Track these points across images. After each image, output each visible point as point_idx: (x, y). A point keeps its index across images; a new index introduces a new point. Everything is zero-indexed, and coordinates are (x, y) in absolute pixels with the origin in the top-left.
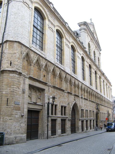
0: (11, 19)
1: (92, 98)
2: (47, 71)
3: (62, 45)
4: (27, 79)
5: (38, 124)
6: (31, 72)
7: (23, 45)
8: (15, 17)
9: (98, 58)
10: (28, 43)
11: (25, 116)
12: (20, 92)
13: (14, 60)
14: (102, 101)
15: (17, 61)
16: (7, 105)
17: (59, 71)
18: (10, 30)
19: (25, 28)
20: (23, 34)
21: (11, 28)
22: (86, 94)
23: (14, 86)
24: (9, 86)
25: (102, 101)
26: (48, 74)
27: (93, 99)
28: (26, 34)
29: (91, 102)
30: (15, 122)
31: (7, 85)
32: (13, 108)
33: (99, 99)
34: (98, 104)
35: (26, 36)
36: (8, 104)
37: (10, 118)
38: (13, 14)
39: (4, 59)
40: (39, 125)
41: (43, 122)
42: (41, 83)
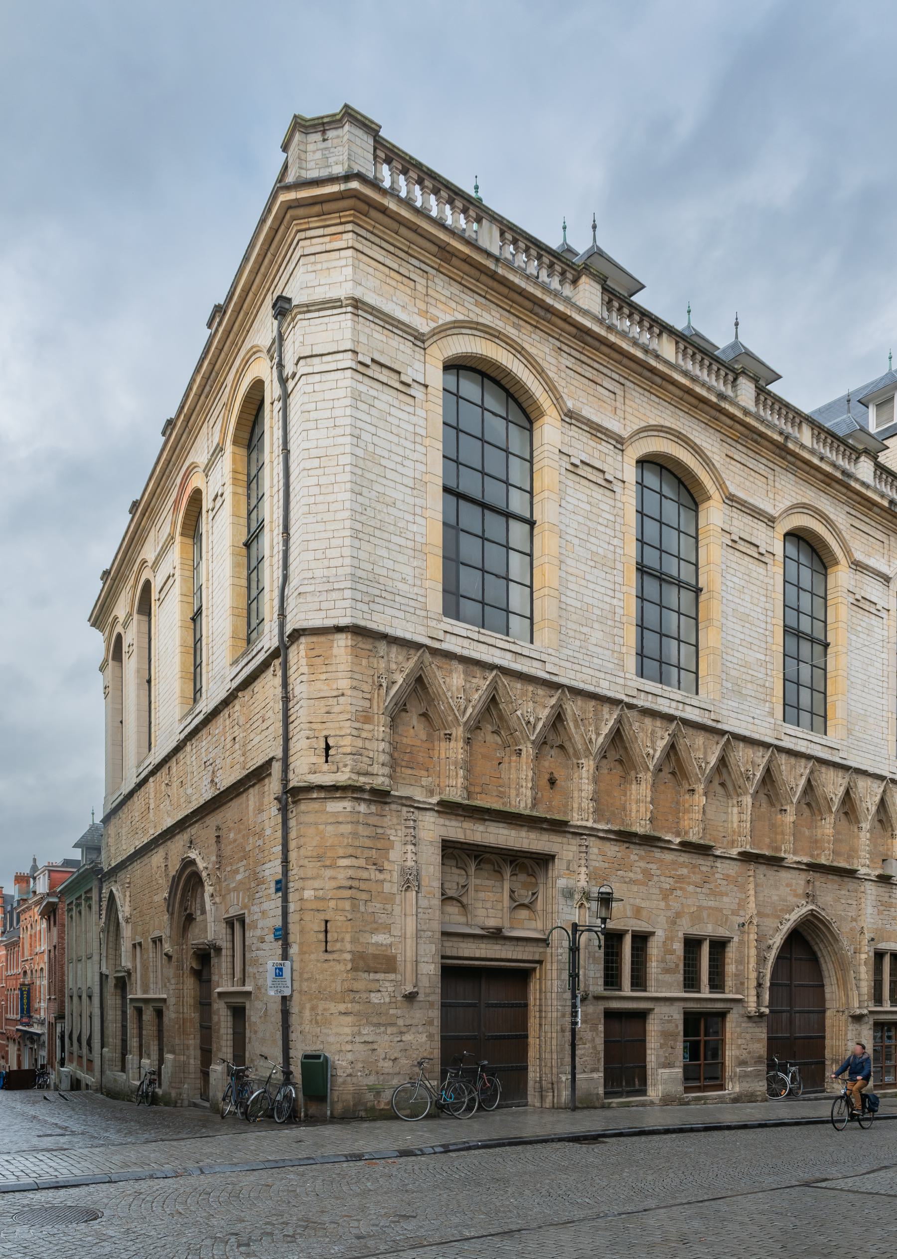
7: (384, 637)
8: (323, 480)
10: (413, 618)
11: (427, 995)
12: (387, 887)
15: (355, 733)
19: (386, 536)
20: (377, 570)
23: (354, 859)
28: (398, 567)
30: (369, 1023)
35: (404, 580)
37: (342, 1007)
42: (522, 826)
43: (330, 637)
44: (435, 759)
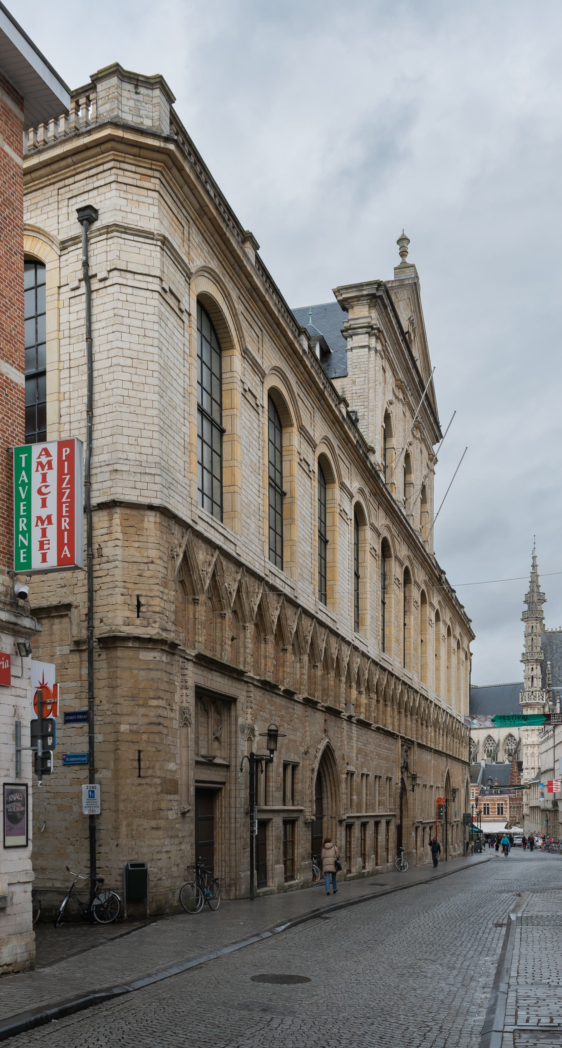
0: (119, 392)
1: (384, 713)
2: (240, 615)
3: (286, 465)
4: (191, 664)
5: (212, 844)
6: (200, 632)
9: (424, 488)
13: (151, 590)
14: (424, 727)
16: (139, 776)
17: (277, 609)
18: (120, 447)
21: (125, 440)
22: (364, 700)
24: (141, 702)
25: (427, 726)
26: (241, 628)
27: (388, 718)
29: (380, 738)
31: (133, 697)
32: (161, 784)
33: (415, 717)
34: (408, 744)
36: (142, 770)
38: (122, 361)
39: (104, 587)
40: (216, 846)
41: (230, 833)
43: (142, 512)
44: (186, 618)
